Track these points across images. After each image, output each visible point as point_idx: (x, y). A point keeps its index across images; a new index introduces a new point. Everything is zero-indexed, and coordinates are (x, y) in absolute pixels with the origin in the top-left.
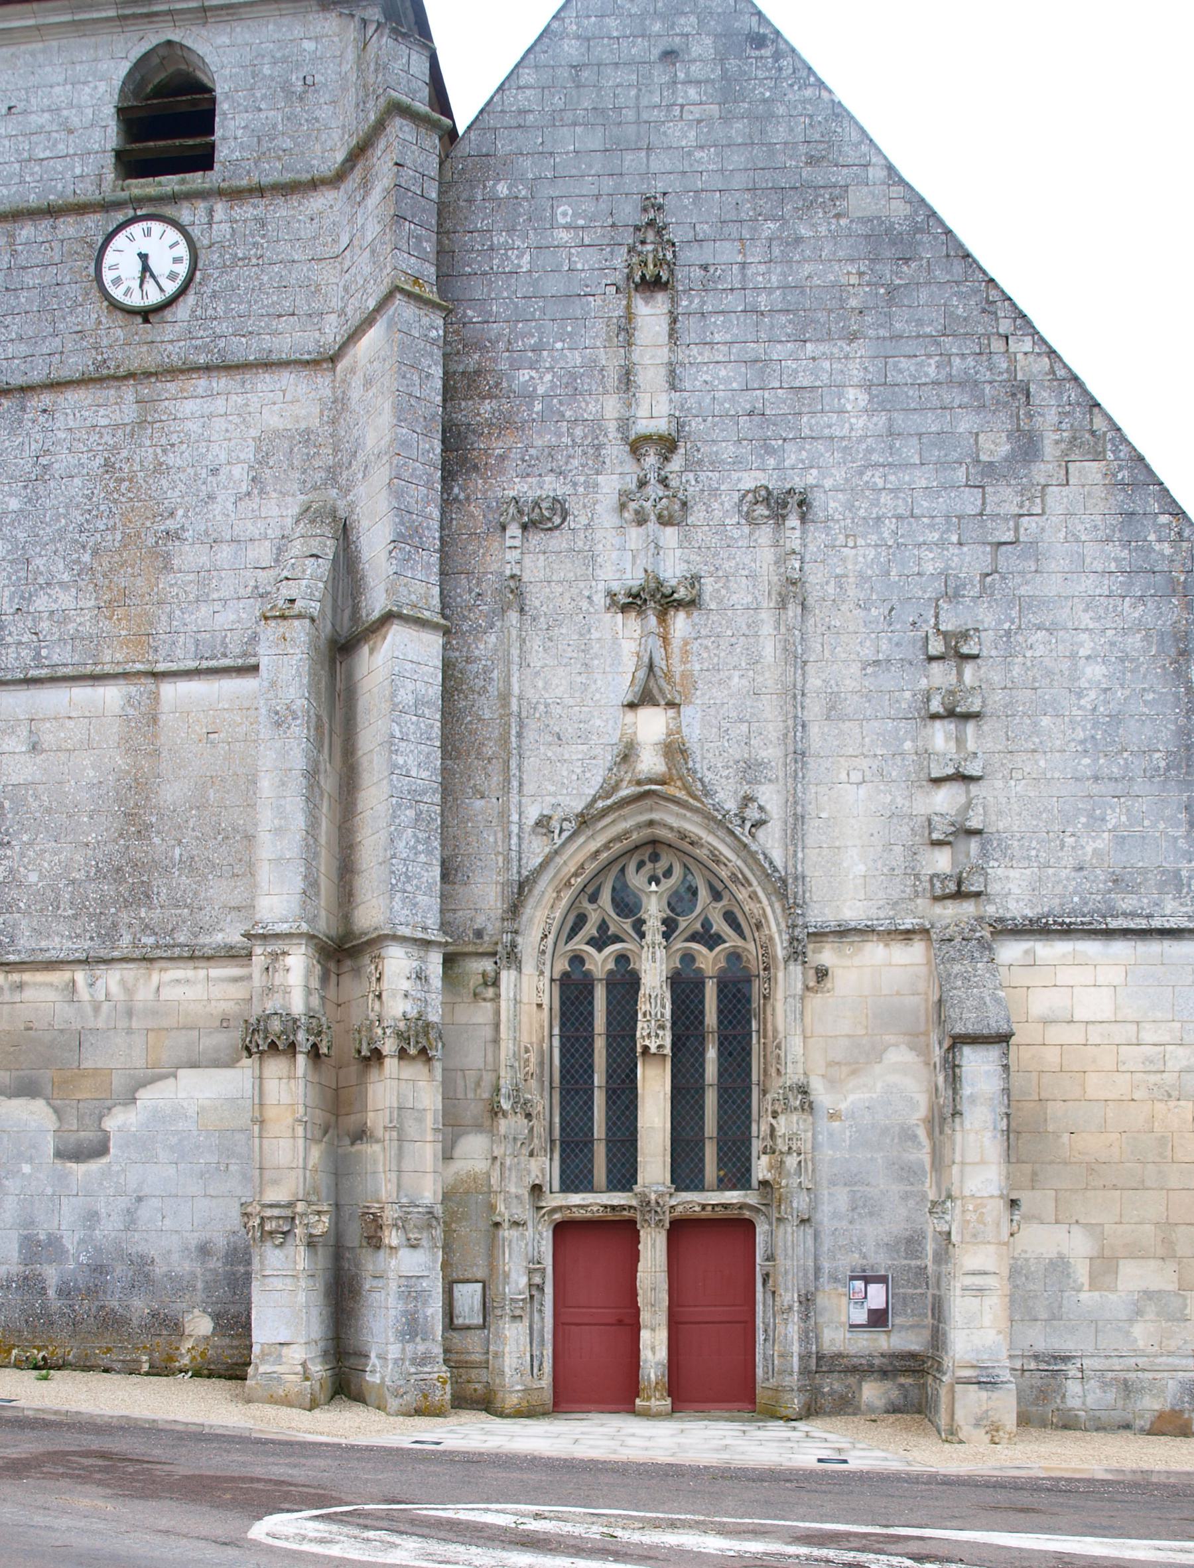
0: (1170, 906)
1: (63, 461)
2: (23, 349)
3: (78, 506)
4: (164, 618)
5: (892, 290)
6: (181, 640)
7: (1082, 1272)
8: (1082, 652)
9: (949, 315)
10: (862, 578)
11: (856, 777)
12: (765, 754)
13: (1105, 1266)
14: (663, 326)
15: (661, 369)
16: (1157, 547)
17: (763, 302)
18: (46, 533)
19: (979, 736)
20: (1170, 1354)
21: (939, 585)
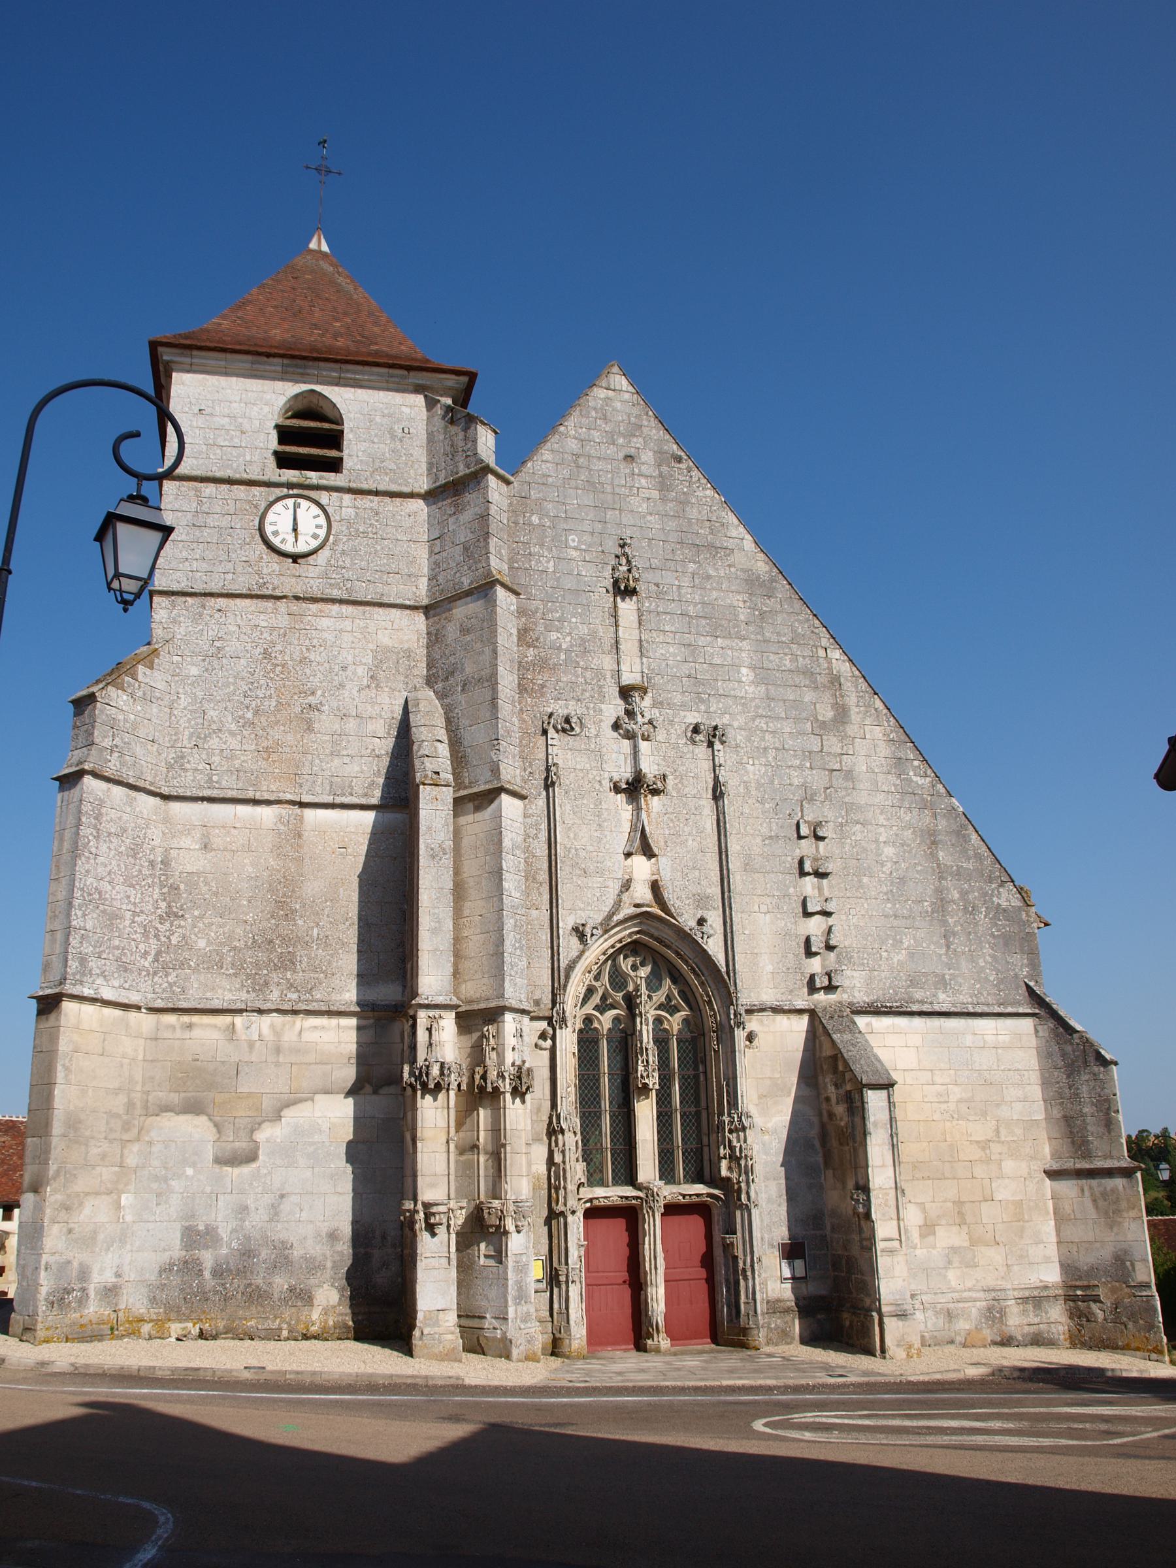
0: (942, 996)
1: (232, 647)
2: (205, 566)
4: (307, 764)
5: (762, 614)
6: (320, 781)
7: (915, 1235)
8: (882, 839)
9: (794, 631)
10: (759, 785)
11: (764, 908)
12: (709, 891)
13: (928, 1229)
14: (634, 617)
15: (637, 643)
16: (915, 779)
17: (691, 610)
18: (219, 694)
19: (830, 887)
20: (970, 1290)
21: (801, 792)
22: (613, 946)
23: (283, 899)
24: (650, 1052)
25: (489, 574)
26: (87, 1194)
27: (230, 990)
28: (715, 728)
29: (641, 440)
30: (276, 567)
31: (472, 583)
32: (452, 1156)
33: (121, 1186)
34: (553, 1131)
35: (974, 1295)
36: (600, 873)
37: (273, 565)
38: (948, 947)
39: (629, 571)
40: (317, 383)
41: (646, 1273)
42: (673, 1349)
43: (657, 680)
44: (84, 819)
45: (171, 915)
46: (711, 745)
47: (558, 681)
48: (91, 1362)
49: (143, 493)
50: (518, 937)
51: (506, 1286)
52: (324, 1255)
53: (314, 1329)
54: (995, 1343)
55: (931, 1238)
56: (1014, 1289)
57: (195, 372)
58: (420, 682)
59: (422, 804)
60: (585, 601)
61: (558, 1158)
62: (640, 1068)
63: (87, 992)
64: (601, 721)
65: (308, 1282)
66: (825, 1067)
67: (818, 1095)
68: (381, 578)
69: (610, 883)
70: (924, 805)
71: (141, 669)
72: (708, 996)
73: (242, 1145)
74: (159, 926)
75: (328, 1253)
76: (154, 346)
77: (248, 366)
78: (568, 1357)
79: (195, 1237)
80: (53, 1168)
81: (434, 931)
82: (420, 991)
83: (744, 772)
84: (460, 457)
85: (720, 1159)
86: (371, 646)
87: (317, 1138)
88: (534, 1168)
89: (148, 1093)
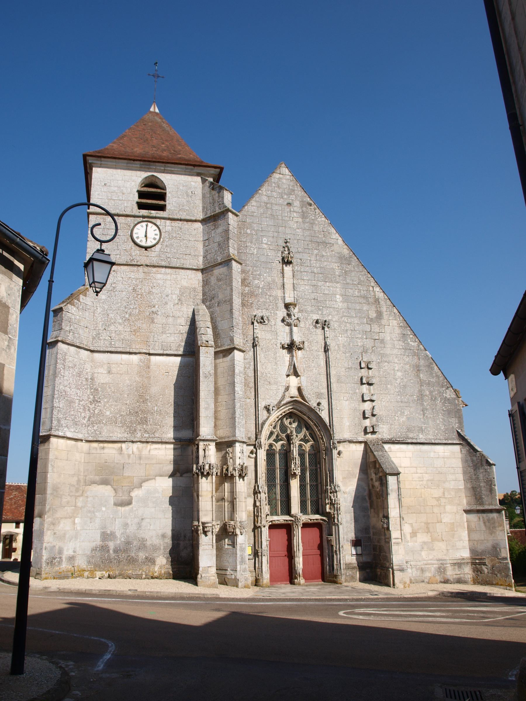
0: (421, 436)
3: (124, 300)
4: (152, 337)
6: (157, 344)
7: (408, 536)
8: (396, 369)
9: (359, 279)
10: (344, 346)
12: (322, 391)
13: (414, 534)
14: (291, 274)
15: (292, 285)
16: (410, 343)
17: (315, 270)
19: (374, 389)
20: (431, 560)
21: (362, 349)
22: (281, 414)
23: (142, 395)
24: (297, 459)
25: (229, 256)
26: (61, 518)
27: (120, 433)
28: (325, 321)
29: (294, 196)
30: (138, 252)
31: (222, 259)
32: (214, 503)
33: (75, 515)
34: (256, 492)
35: (433, 562)
36: (276, 383)
37: (137, 251)
38: (424, 415)
39: (289, 253)
40: (155, 172)
41: (294, 552)
42: (306, 584)
43: (301, 300)
44: (58, 361)
45: (95, 401)
46: (323, 328)
47: (258, 301)
48: (65, 587)
49: (103, 248)
50: (241, 411)
51: (236, 557)
52: (160, 544)
53: (156, 574)
54: (441, 582)
55: (415, 538)
56: (450, 560)
57: (103, 167)
58: (199, 301)
59: (201, 355)
60: (270, 267)
61: (258, 504)
62: (293, 466)
63: (61, 434)
64: (277, 318)
65: (153, 555)
66: (371, 466)
67: (368, 478)
68: (183, 257)
69: (280, 388)
70: (414, 354)
71: (81, 296)
72: (321, 435)
73: (125, 498)
74: (90, 406)
75: (162, 543)
76: (85, 156)
77: (125, 165)
78: (262, 587)
79: (106, 536)
80: (47, 507)
81: (206, 409)
82: (200, 434)
83: (337, 340)
84: (216, 204)
85: (326, 504)
86: (179, 286)
87: (157, 495)
88: (248, 508)
89: (86, 476)
